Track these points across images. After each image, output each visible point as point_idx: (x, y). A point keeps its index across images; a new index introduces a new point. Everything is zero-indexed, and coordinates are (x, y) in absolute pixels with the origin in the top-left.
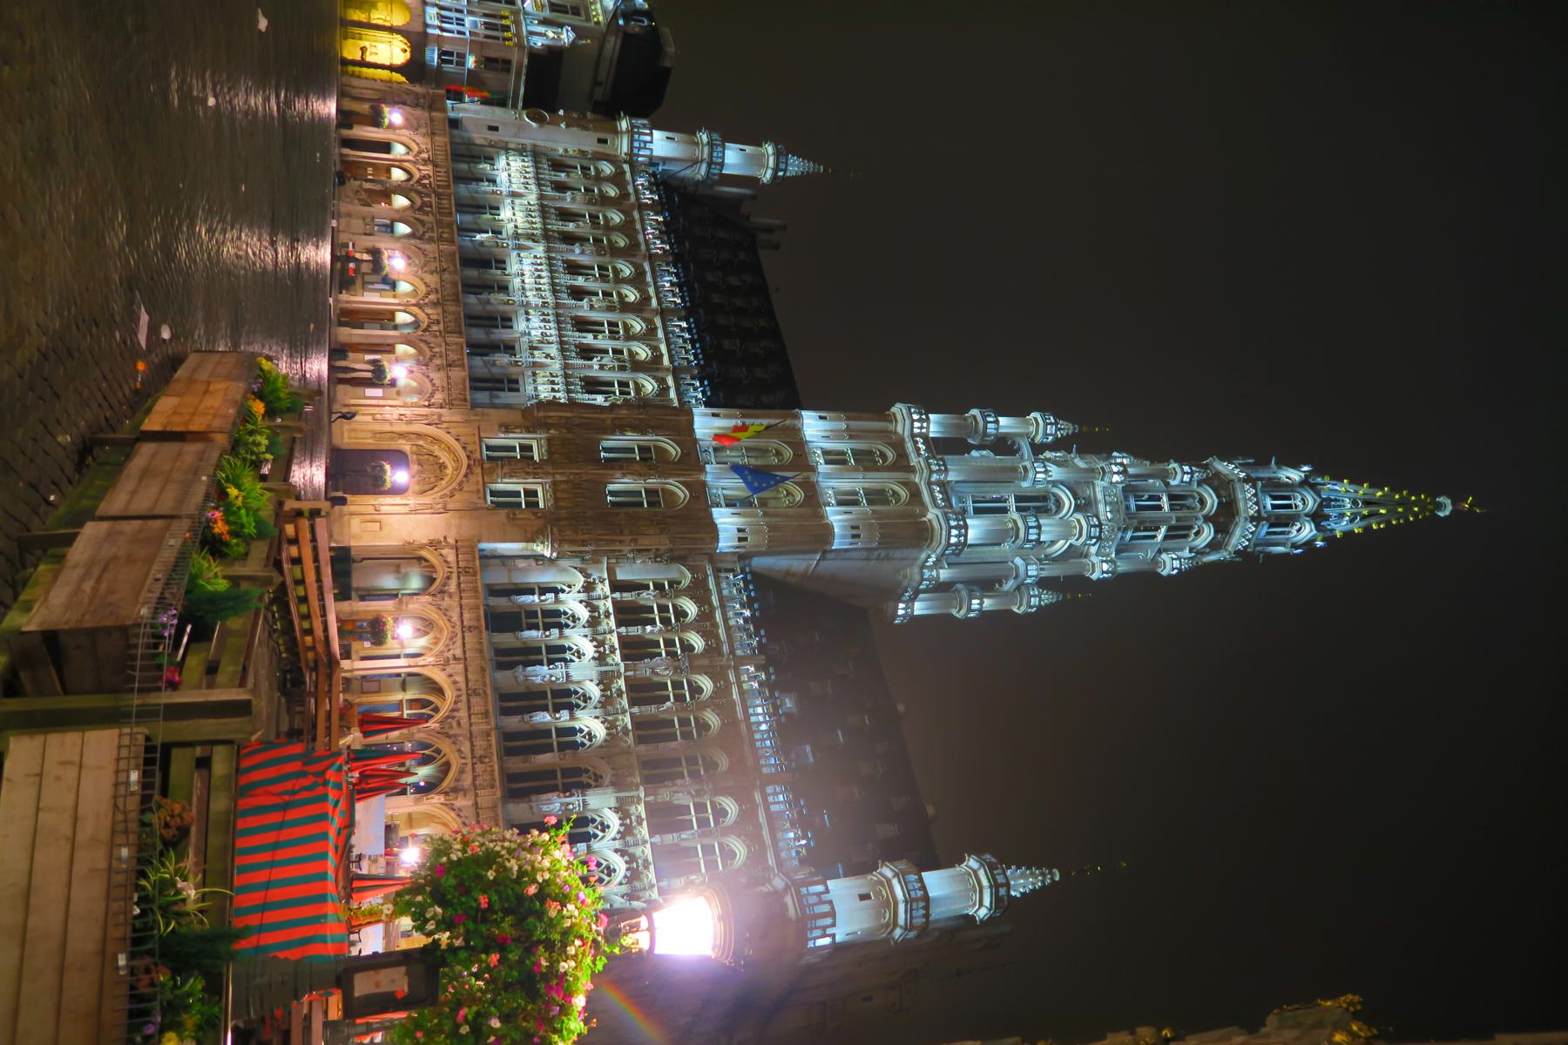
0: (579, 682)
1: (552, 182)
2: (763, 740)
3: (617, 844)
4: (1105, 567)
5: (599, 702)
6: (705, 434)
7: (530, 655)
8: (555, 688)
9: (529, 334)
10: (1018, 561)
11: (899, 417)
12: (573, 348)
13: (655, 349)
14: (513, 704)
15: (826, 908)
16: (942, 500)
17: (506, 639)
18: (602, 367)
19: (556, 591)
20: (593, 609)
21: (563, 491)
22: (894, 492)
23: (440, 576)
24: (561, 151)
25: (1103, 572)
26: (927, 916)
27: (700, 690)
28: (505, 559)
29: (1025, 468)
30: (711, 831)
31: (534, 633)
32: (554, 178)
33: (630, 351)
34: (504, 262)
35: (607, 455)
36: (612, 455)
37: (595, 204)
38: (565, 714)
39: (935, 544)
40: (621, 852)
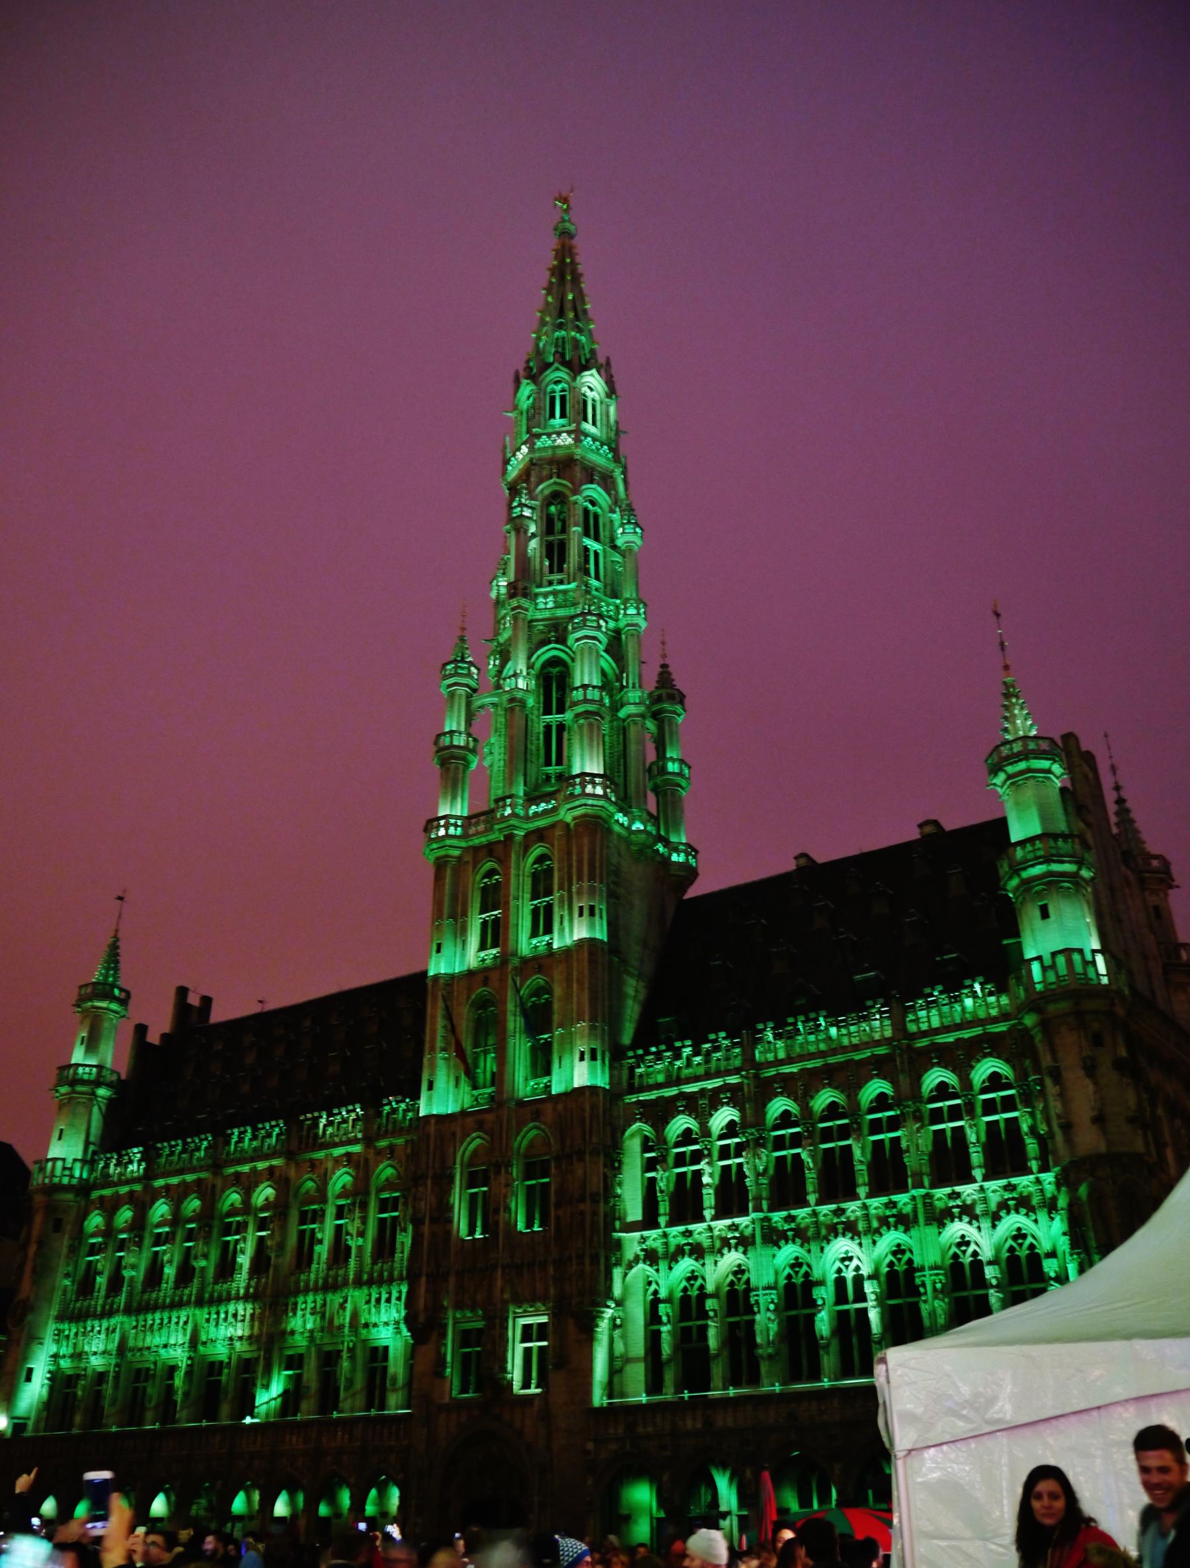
0: (776, 1273)
1: (107, 1296)
2: (849, 1034)
3: (986, 1224)
4: (632, 611)
5: (802, 1246)
6: (456, 1101)
8: (782, 1305)
9: (311, 1331)
10: (622, 714)
11: (442, 853)
12: (332, 1273)
13: (337, 1162)
14: (805, 1362)
15: (1061, 960)
16: (548, 802)
18: (361, 1234)
19: (656, 1302)
20: (680, 1252)
24: (67, 1282)
25: (638, 614)
26: (1065, 837)
27: (786, 1114)
28: (615, 1370)
29: (512, 700)
30: (966, 1104)
31: (712, 1333)
32: (103, 1293)
33: (339, 1196)
34: (212, 1364)
35: (479, 1230)
36: (479, 1223)
37: (141, 1238)
38: (819, 1294)
39: (603, 814)
40: (996, 1218)
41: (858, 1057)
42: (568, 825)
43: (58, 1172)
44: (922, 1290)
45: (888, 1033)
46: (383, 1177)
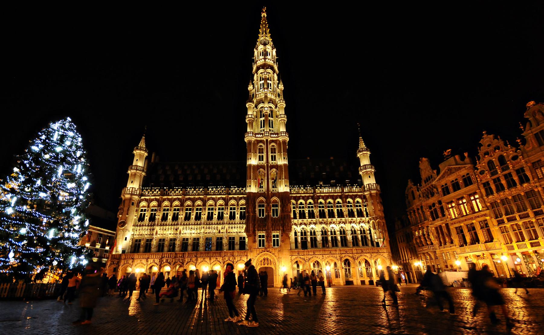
3: (358, 224)
11: (251, 139)
13: (219, 199)
16: (275, 135)
17: (309, 245)
18: (227, 214)
21: (275, 228)
23: (298, 259)
24: (136, 217)
26: (369, 165)
33: (219, 206)
40: (359, 223)
41: (335, 194)
42: (280, 141)
45: (341, 191)
46: (231, 203)
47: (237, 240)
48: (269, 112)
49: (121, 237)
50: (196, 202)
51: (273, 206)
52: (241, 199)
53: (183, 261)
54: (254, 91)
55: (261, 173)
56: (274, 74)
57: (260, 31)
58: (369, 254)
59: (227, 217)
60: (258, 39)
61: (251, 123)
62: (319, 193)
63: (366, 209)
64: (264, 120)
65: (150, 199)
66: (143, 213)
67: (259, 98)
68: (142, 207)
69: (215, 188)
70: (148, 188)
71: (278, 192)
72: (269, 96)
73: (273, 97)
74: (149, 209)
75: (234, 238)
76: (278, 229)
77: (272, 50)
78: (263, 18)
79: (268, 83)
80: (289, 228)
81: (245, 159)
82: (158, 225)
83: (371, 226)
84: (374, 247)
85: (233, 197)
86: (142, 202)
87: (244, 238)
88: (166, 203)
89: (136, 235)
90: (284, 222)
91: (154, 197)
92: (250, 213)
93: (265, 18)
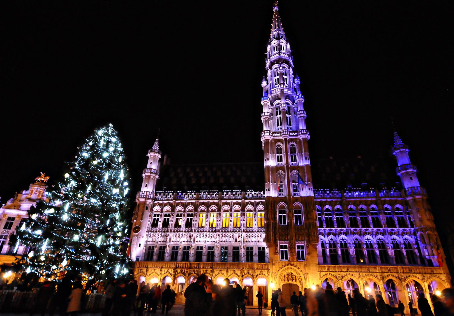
7: (346, 253)
13: (235, 203)
16: (295, 133)
18: (244, 221)
21: (299, 238)
22: (291, 145)
23: (329, 276)
24: (149, 223)
40: (402, 236)
42: (300, 139)
43: (148, 195)
44: (388, 248)
46: (247, 208)
47: (256, 251)
48: (286, 108)
49: (136, 244)
50: (211, 207)
51: (296, 212)
52: (258, 203)
53: (198, 272)
54: (268, 87)
55: (281, 175)
56: (289, 68)
57: (273, 26)
58: (420, 275)
59: (244, 224)
60: (271, 33)
61: (267, 121)
62: (348, 198)
63: (409, 218)
64: (280, 118)
65: (163, 203)
66: (156, 218)
67: (274, 94)
68: (155, 212)
69: (230, 192)
70: (161, 192)
71: (301, 197)
72: (286, 91)
73: (290, 93)
74: (162, 214)
75: (252, 248)
76: (303, 239)
77: (287, 43)
78: (275, 12)
79: (284, 78)
80: (316, 238)
81: (262, 160)
82: (171, 231)
83: (419, 239)
84: (426, 266)
85: (250, 202)
86: (156, 207)
87: (263, 248)
88: (180, 208)
89: (149, 241)
90: (310, 231)
91: (167, 202)
92: (270, 220)
93: (277, 12)
